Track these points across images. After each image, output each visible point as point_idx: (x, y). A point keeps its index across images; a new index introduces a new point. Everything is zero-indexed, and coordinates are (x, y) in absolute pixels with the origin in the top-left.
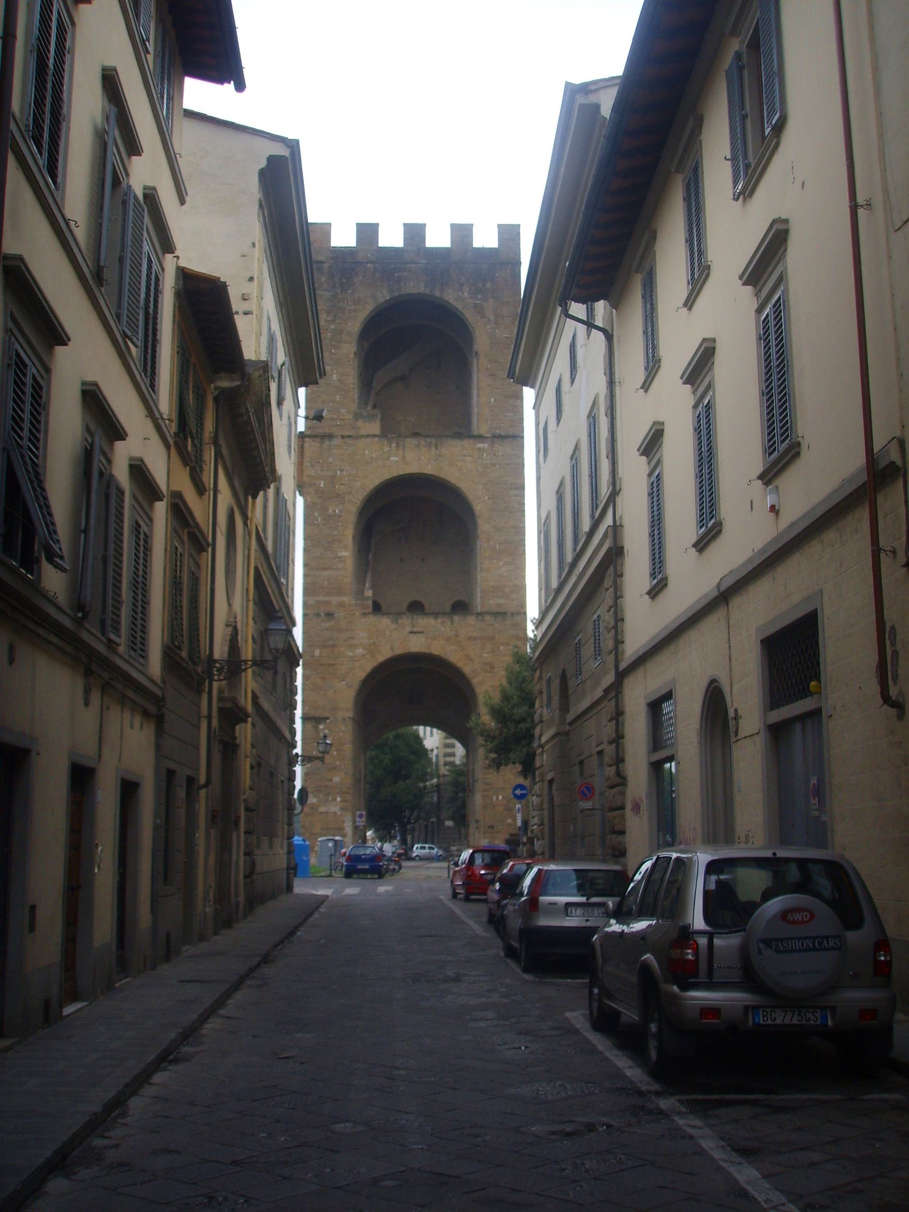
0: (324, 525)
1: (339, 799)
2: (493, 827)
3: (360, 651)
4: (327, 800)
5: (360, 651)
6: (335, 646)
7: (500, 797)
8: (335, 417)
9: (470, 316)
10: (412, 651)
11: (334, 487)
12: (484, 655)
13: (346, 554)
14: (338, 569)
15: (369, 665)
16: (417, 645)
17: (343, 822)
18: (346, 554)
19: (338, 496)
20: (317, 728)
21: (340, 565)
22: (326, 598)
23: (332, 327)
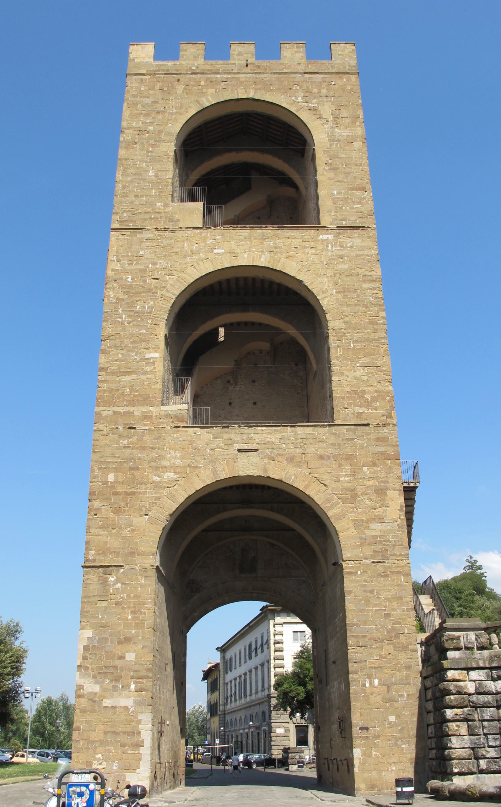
0: (129, 323)
1: (133, 686)
2: (367, 729)
4: (115, 688)
5: (170, 475)
6: (137, 469)
7: (376, 682)
8: (149, 210)
9: (305, 116)
10: (241, 474)
11: (145, 281)
12: (342, 479)
13: (157, 355)
14: (145, 373)
15: (182, 494)
16: (249, 467)
17: (139, 722)
18: (157, 355)
19: (149, 290)
20: (106, 580)
21: (148, 369)
22: (127, 409)
23: (151, 128)
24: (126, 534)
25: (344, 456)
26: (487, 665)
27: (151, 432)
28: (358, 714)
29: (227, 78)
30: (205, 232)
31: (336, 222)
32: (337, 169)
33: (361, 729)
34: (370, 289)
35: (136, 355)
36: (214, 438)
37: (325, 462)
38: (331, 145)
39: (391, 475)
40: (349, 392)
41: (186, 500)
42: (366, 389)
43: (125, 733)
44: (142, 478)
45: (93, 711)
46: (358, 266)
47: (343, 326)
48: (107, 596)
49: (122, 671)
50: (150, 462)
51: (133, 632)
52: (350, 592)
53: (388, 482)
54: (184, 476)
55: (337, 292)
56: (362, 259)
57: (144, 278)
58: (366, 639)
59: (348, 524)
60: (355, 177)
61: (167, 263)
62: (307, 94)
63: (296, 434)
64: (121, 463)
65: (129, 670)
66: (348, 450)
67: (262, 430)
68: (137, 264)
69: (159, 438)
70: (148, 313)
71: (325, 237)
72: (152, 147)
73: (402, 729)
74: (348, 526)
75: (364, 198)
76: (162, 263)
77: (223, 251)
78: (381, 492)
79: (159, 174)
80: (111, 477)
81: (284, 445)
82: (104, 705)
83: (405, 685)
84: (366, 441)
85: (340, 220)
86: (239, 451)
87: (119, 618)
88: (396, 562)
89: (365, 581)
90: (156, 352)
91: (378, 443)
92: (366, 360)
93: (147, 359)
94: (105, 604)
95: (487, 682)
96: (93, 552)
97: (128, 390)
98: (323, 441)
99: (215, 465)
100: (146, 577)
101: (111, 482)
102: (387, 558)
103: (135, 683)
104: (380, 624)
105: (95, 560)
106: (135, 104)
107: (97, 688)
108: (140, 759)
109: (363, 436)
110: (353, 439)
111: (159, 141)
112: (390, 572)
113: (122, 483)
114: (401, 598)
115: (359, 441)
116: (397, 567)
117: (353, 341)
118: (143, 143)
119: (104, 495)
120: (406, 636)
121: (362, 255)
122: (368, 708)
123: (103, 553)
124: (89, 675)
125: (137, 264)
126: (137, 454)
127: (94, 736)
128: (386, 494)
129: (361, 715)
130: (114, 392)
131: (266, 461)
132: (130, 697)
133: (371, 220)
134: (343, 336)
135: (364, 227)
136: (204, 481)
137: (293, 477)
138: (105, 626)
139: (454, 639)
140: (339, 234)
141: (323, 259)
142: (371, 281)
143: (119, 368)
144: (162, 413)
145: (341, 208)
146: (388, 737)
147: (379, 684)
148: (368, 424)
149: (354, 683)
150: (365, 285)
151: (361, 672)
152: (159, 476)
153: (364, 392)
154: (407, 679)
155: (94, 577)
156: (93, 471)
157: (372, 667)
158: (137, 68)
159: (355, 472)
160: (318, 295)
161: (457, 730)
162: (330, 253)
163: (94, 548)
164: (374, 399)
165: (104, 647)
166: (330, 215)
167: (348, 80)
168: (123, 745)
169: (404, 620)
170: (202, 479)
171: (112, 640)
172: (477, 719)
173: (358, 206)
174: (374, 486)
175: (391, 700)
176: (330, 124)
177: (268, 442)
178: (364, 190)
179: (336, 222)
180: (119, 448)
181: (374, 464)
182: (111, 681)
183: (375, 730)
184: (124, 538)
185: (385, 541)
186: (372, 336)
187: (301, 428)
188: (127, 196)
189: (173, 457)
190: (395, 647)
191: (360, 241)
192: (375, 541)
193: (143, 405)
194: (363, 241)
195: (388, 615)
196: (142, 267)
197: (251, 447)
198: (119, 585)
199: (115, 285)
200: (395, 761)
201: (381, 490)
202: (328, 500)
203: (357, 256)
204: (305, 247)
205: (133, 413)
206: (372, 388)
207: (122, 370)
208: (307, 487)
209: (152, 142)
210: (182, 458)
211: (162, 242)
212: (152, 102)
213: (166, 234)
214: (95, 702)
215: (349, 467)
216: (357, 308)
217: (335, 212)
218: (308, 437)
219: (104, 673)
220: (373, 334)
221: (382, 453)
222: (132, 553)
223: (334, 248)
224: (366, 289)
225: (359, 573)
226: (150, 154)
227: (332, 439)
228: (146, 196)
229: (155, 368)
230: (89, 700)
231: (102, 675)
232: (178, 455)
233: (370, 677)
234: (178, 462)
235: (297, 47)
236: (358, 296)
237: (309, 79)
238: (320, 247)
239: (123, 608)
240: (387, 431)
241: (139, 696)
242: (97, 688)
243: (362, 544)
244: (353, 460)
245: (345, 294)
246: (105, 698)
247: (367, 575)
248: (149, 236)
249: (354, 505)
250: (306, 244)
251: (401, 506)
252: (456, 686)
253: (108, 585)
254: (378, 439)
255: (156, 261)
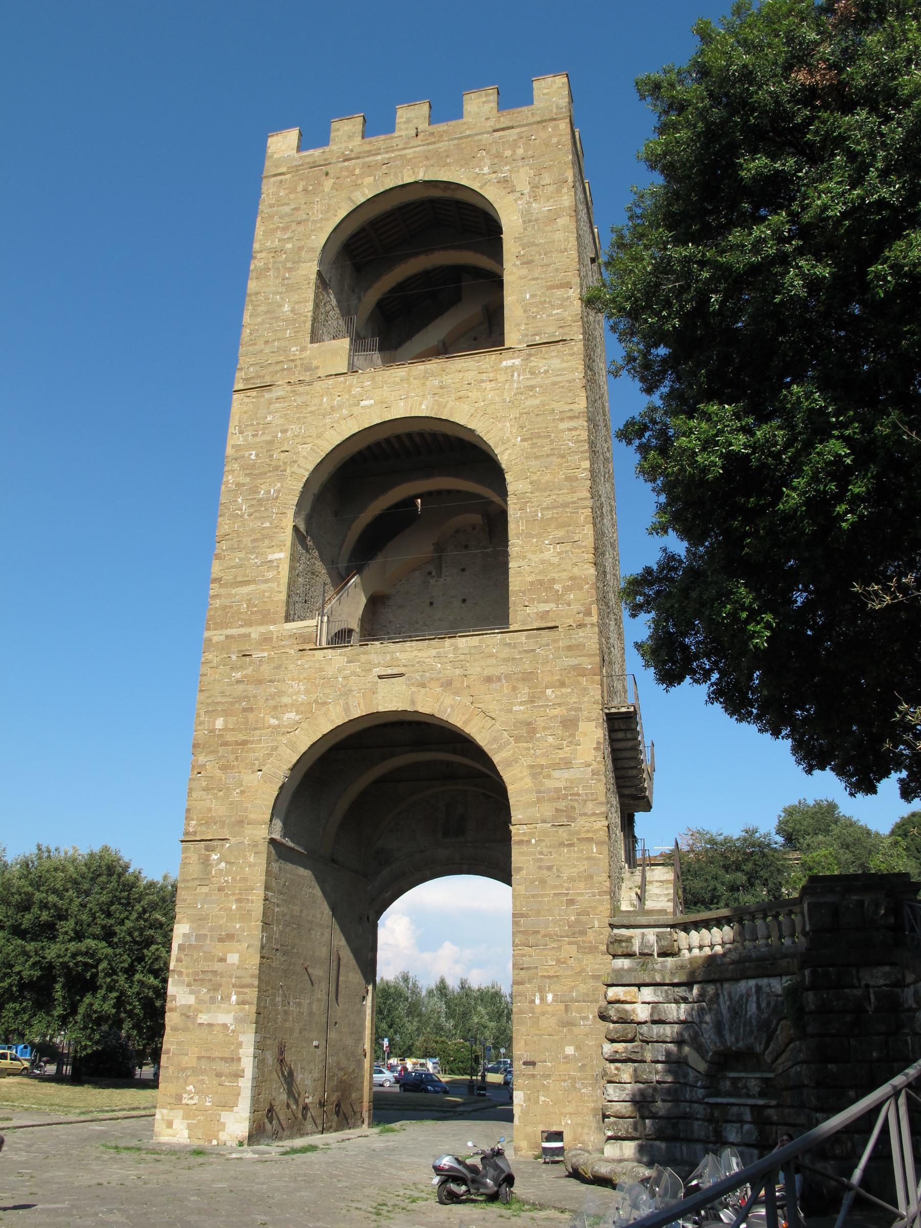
0: (250, 515)
1: (234, 998)
2: (533, 1064)
3: (291, 716)
4: (213, 1000)
5: (291, 716)
6: (251, 710)
7: (550, 997)
8: (282, 358)
9: (492, 194)
10: (381, 709)
12: (515, 708)
13: (282, 555)
14: (266, 581)
15: (305, 740)
16: (392, 699)
17: (240, 1045)
18: (282, 555)
19: (276, 468)
21: (270, 575)
22: (243, 630)
23: (289, 246)
24: (234, 797)
25: (520, 675)
26: (667, 981)
27: (270, 659)
28: (522, 1043)
29: (389, 158)
30: (352, 379)
31: (526, 339)
32: (533, 261)
33: (525, 1063)
34: (570, 430)
35: (256, 558)
36: (349, 662)
37: (495, 686)
38: (525, 229)
39: (586, 699)
40: (532, 583)
41: (309, 748)
42: (556, 576)
43: (222, 1059)
44: (257, 721)
45: (186, 1029)
46: (555, 398)
47: (529, 488)
48: (209, 879)
49: (222, 977)
50: (267, 700)
51: (238, 926)
52: (520, 869)
53: (580, 709)
54: (308, 716)
55: (522, 440)
56: (560, 387)
57: (271, 453)
58: (539, 936)
59: (521, 772)
60: (557, 270)
61: (300, 428)
62: (496, 160)
63: (456, 648)
64: (232, 703)
65: (231, 977)
66: (526, 666)
67: (411, 647)
68: (264, 433)
69: (278, 667)
70: (274, 499)
71: (509, 363)
72: (289, 272)
73: (584, 1066)
74: (520, 775)
75: (568, 298)
76: (294, 428)
77: (372, 402)
78: (570, 724)
79: (296, 307)
80: (219, 723)
81: (439, 665)
82: (199, 1021)
83: (591, 1002)
84: (553, 651)
85: (532, 335)
86: (380, 677)
87: (221, 908)
88: (587, 824)
89: (541, 853)
90: (281, 551)
91: (569, 653)
92: (560, 533)
93: (270, 561)
94: (205, 890)
95: (665, 1005)
96: (194, 822)
97: (245, 606)
98: (491, 655)
99: (347, 698)
100: (256, 853)
101: (220, 730)
102: (572, 819)
103: (237, 993)
104: (560, 915)
105: (196, 833)
106: (271, 217)
107: (191, 1000)
108: (239, 1094)
109: (548, 645)
110: (533, 650)
111: (299, 262)
112: (578, 839)
113: (233, 730)
114: (591, 877)
115: (542, 652)
116: (588, 831)
117: (542, 509)
118: (278, 268)
119: (209, 747)
120: (596, 932)
121: (560, 382)
122: (536, 1035)
123: (206, 822)
124: (183, 982)
125: (264, 433)
126: (252, 689)
127: (186, 1061)
128: (576, 726)
129: (526, 1044)
130: (228, 610)
131: (414, 689)
132: (230, 1012)
133: (575, 329)
134: (528, 502)
135: (565, 340)
136: (332, 722)
137: (449, 710)
138: (204, 919)
139: (624, 941)
140: (530, 355)
141: (506, 394)
142: (571, 418)
143: (235, 578)
144: (285, 633)
145: (535, 317)
146: (563, 1077)
147: (554, 1000)
148: (557, 627)
149: (519, 998)
150: (562, 426)
151: (530, 982)
152: (277, 718)
153: (553, 581)
154: (594, 994)
155: (194, 853)
156: (198, 715)
157: (545, 976)
158: (276, 166)
159: (534, 697)
160: (496, 447)
161: (616, 1075)
162: (515, 385)
163: (195, 818)
164: (568, 589)
165: (203, 946)
166: (519, 330)
167: (555, 128)
168: (219, 1075)
169: (595, 908)
170: (332, 718)
171: (211, 937)
172: (649, 1059)
173: (559, 311)
174: (561, 716)
175: (570, 1024)
176: (526, 198)
177: (418, 662)
178: (568, 285)
179: (526, 339)
180: (230, 684)
181: (562, 684)
182: (209, 990)
183: (545, 1066)
184: (231, 803)
185: (571, 795)
186: (569, 499)
187: (464, 639)
188: (255, 344)
189: (296, 691)
190: (579, 947)
191: (559, 361)
192: (557, 796)
193: (262, 624)
194: (563, 361)
195: (571, 902)
196: (269, 438)
197: (395, 671)
198: (223, 864)
199: (236, 466)
200: (571, 1111)
201: (571, 721)
202: (495, 740)
203: (554, 384)
204: (482, 381)
205: (249, 635)
206: (565, 574)
207: (239, 579)
208: (466, 723)
209: (289, 265)
210: (307, 692)
211: (295, 400)
212: (293, 209)
213: (301, 389)
214: (188, 1017)
215: (526, 690)
216: (549, 460)
217: (526, 324)
218: (473, 651)
219: (201, 980)
220: (569, 496)
221: (574, 668)
222: (240, 823)
223: (521, 377)
224: (563, 431)
225: (533, 841)
226: (286, 282)
227: (506, 652)
228: (279, 340)
229: (279, 573)
230: (182, 1014)
231: (199, 983)
232: (302, 688)
233: (541, 990)
234: (302, 698)
235: (486, 95)
236: (552, 442)
237: (500, 138)
238: (502, 378)
239: (227, 895)
240: (581, 634)
241: (241, 1010)
242: (191, 1000)
243: (539, 800)
244: (533, 680)
245: (534, 441)
246: (201, 1012)
247: (544, 844)
248: (280, 393)
249: (531, 745)
250: (484, 377)
251: (598, 743)
252: (618, 1011)
253: (210, 865)
254: (569, 648)
255: (287, 427)
